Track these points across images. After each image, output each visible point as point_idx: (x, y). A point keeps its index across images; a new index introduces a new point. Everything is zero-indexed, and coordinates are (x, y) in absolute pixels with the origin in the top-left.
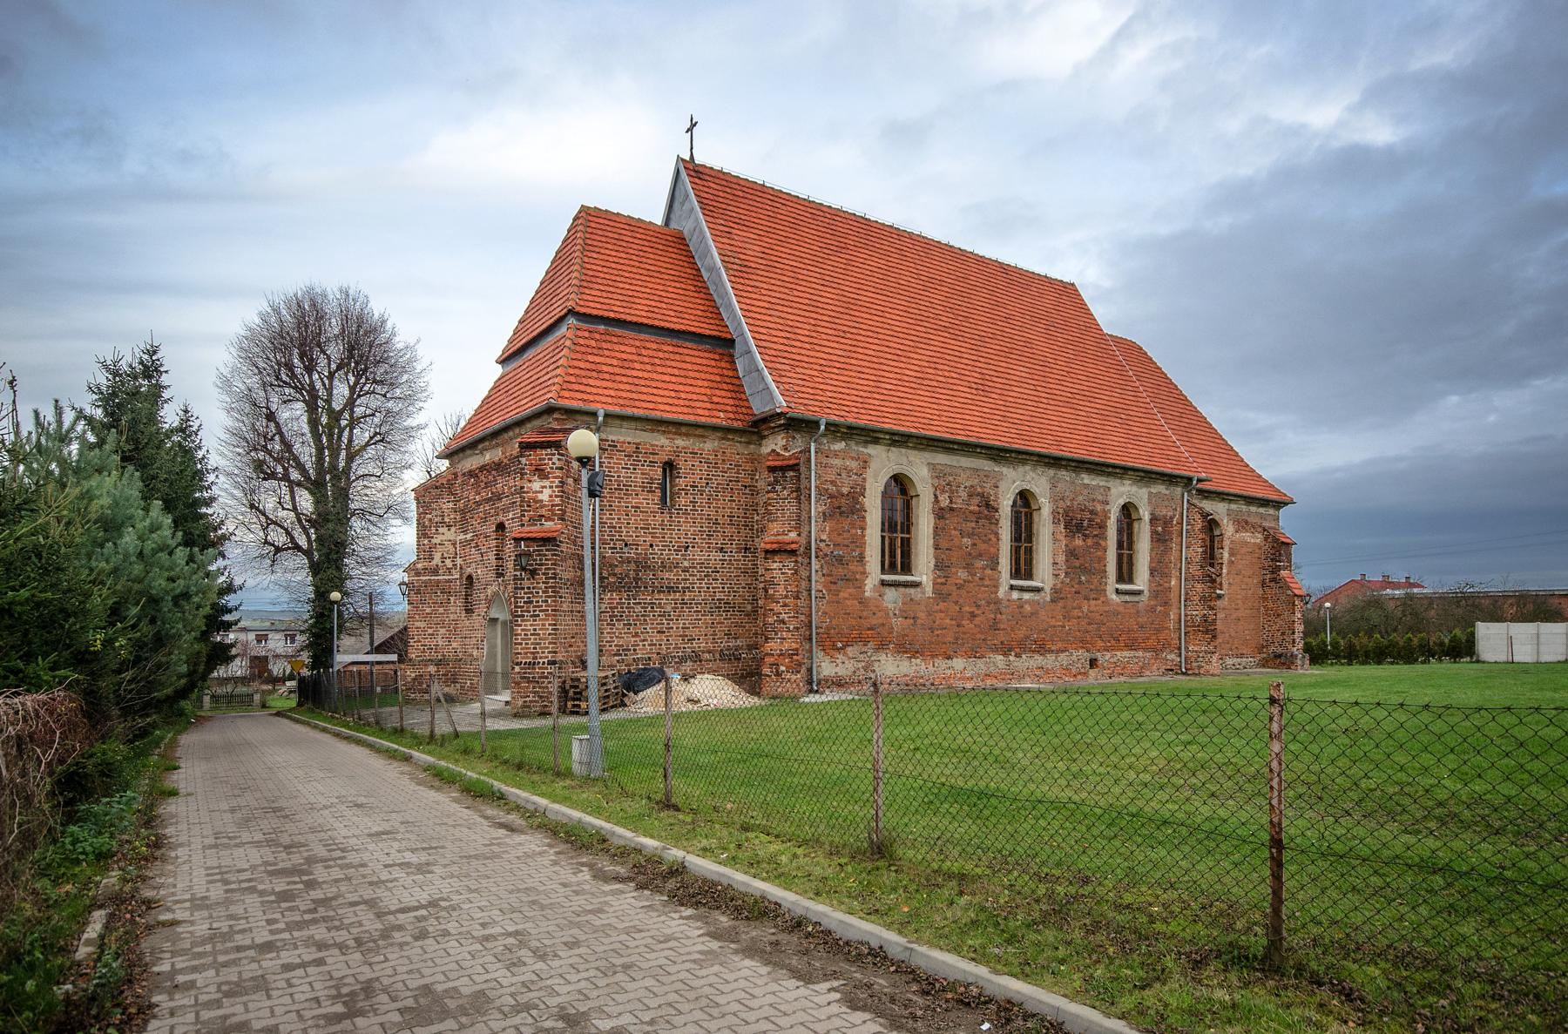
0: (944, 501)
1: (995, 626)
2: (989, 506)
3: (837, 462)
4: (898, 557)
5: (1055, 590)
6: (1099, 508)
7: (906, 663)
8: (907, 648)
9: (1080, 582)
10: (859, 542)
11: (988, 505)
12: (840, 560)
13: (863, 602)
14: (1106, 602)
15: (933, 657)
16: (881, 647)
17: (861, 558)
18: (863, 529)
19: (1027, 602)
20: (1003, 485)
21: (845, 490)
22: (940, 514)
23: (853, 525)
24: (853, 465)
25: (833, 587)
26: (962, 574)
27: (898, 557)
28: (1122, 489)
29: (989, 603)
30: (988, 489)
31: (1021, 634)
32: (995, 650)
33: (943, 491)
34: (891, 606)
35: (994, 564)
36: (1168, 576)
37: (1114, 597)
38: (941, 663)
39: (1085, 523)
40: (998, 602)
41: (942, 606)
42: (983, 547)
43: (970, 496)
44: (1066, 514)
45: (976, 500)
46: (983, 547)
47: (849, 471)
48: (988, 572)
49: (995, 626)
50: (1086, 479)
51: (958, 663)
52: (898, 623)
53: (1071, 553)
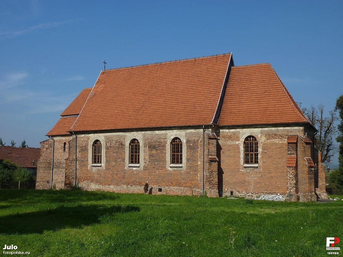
0: (108, 145)
1: (124, 177)
2: (122, 145)
3: (82, 139)
4: (97, 159)
5: (145, 167)
6: (162, 140)
7: (98, 186)
8: (97, 182)
9: (155, 164)
10: (87, 157)
11: (122, 144)
12: (82, 161)
13: (88, 171)
14: (167, 170)
15: (105, 185)
16: (92, 181)
17: (87, 160)
18: (88, 154)
19: (135, 170)
20: (126, 139)
21: (84, 145)
22: (107, 148)
23: (85, 153)
24: (86, 139)
25: (81, 167)
26: (114, 163)
27: (97, 159)
28: (173, 133)
29: (122, 171)
30: (122, 140)
31: (133, 179)
32: (124, 184)
33: (108, 142)
34: (94, 171)
35: (124, 160)
36: (196, 161)
37: (170, 169)
38: (107, 186)
39: (157, 146)
40: (125, 170)
41: (108, 171)
42: (120, 156)
43: (116, 142)
44: (149, 144)
45: (118, 143)
46: (120, 156)
47: (85, 141)
48: (122, 162)
49: (124, 177)
50: (157, 132)
51: (112, 187)
52: (96, 176)
53: (151, 156)
